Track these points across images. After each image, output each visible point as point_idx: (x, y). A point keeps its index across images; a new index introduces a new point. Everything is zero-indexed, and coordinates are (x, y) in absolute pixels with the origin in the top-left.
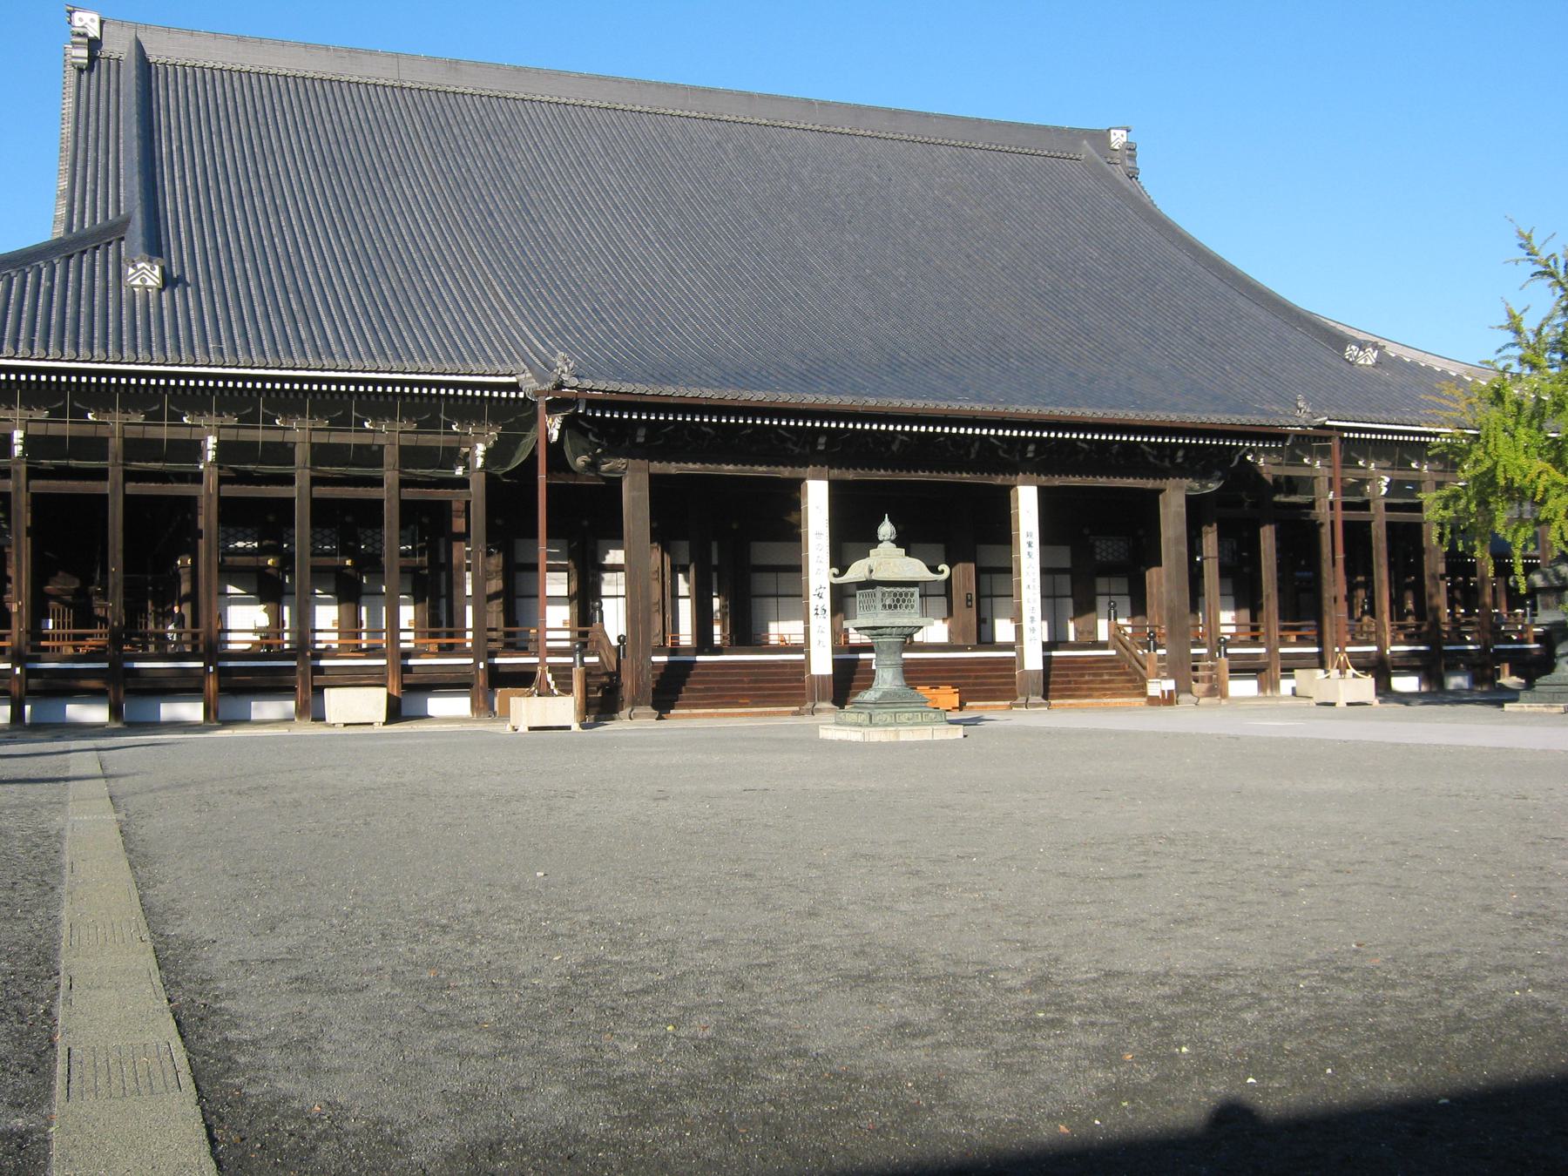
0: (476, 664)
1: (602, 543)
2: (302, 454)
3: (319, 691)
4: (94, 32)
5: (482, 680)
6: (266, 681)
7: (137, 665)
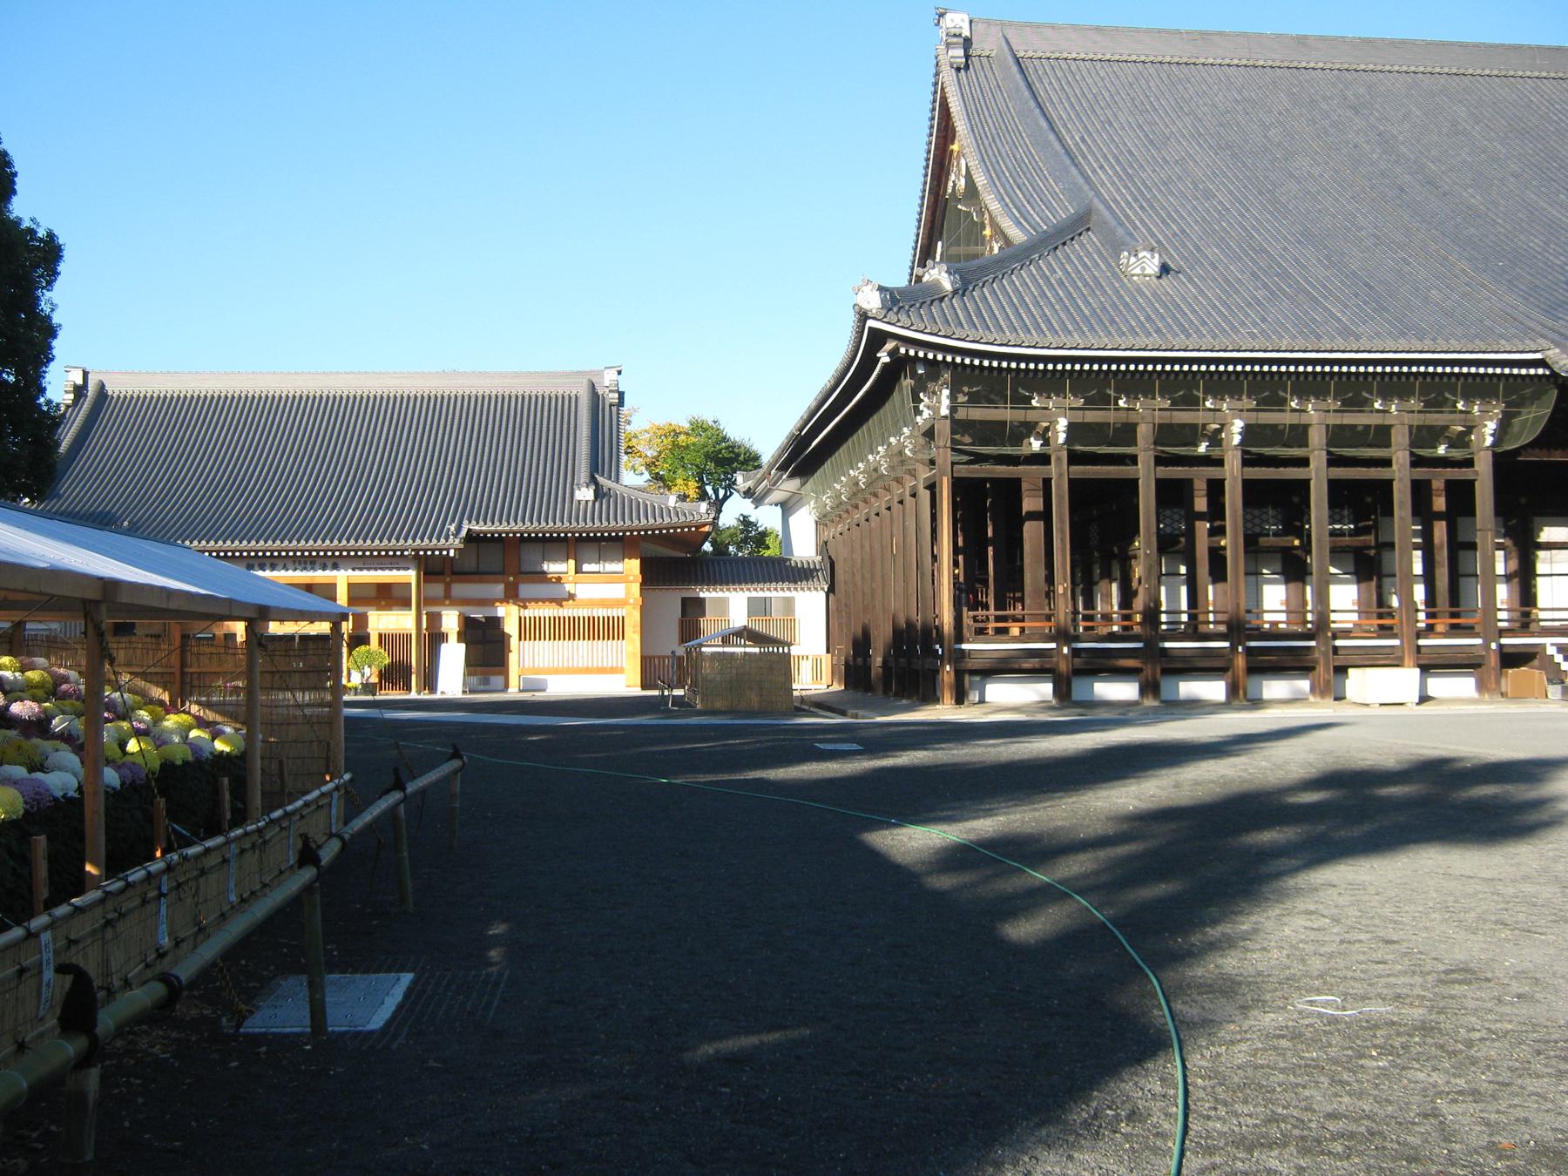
0: (1486, 646)
1: (1537, 520)
2: (1317, 437)
3: (1341, 670)
4: (966, 33)
5: (1494, 661)
6: (1288, 660)
7: (1168, 645)
